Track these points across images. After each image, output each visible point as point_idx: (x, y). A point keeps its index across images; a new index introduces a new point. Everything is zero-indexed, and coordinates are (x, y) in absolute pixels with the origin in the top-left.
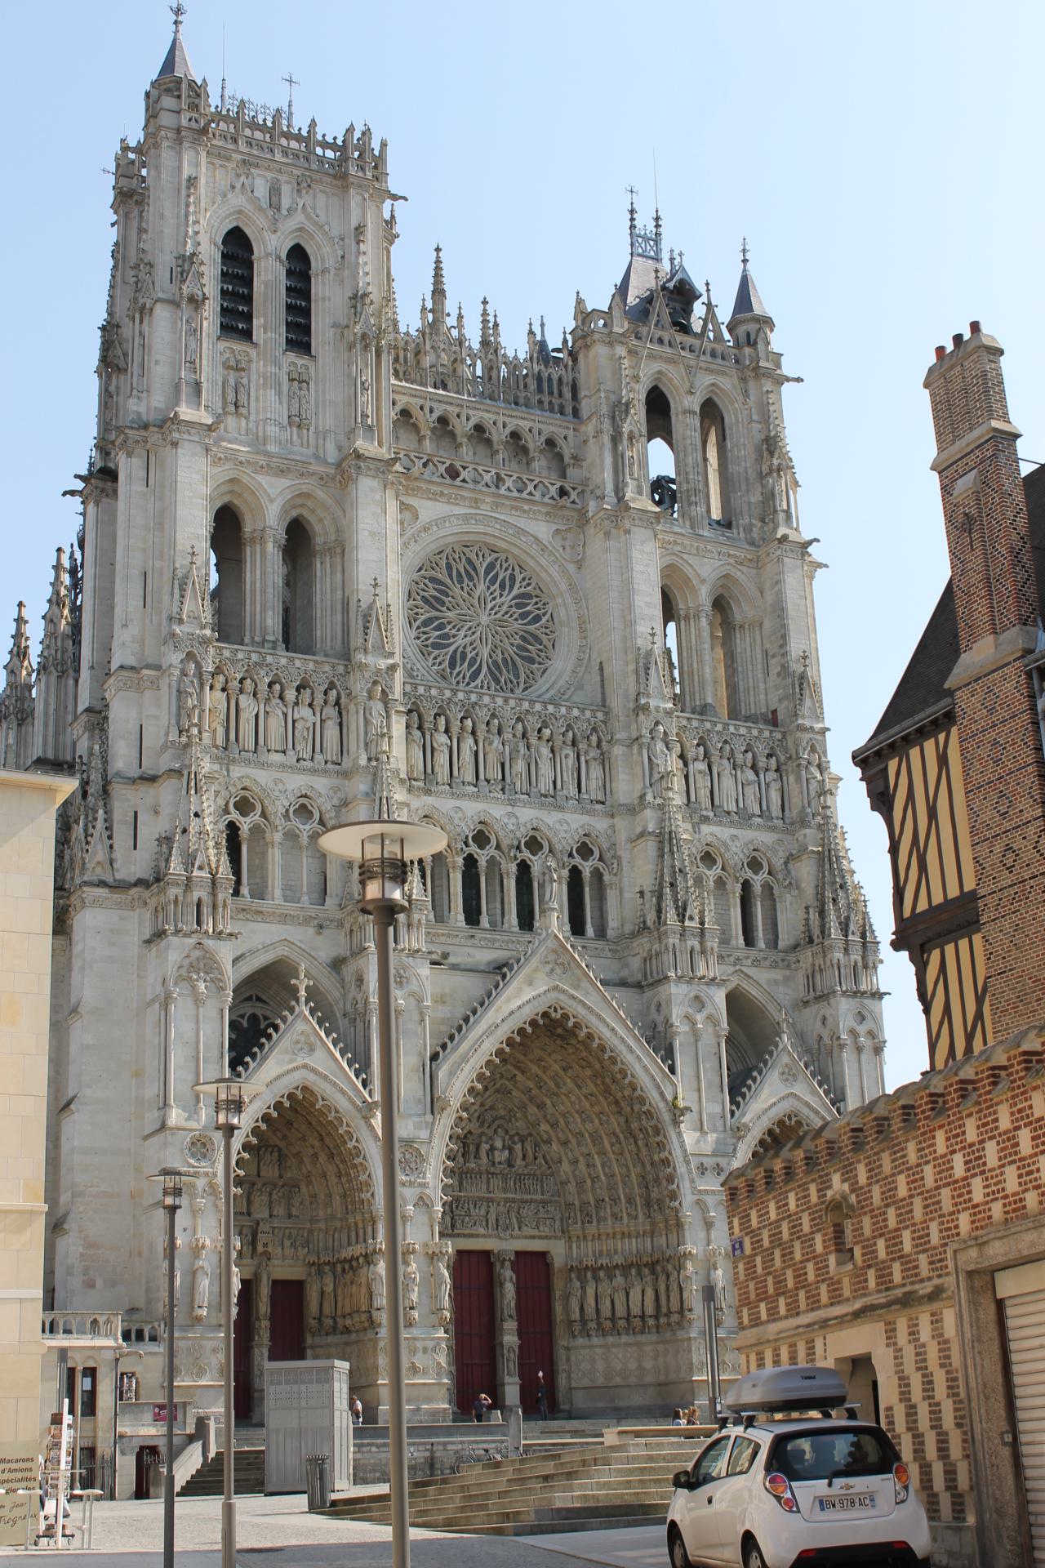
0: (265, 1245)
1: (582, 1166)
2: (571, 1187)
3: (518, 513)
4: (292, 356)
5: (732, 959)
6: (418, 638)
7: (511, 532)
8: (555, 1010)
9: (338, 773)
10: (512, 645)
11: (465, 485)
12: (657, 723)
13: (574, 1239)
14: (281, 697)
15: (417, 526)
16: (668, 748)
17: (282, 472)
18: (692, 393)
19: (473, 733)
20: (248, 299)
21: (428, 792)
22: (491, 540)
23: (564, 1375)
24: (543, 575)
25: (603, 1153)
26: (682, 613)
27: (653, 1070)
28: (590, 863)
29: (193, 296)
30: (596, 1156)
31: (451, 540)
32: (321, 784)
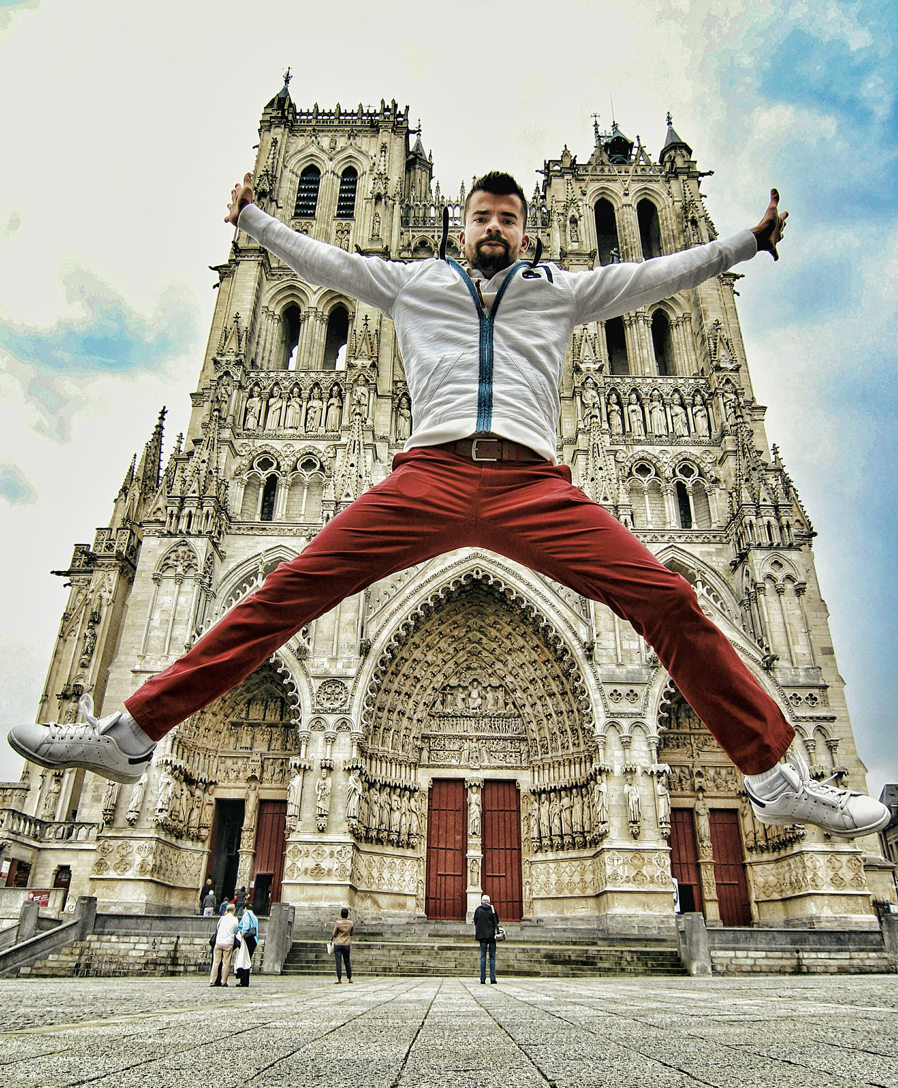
0: (254, 771)
1: (539, 707)
2: (533, 726)
4: (340, 220)
5: (666, 538)
8: (478, 573)
9: (334, 436)
12: (587, 379)
13: (536, 769)
14: (299, 396)
16: (598, 394)
18: (626, 195)
20: (315, 199)
23: (528, 887)
25: (552, 695)
27: (567, 614)
29: (263, 190)
30: (547, 698)
32: (321, 446)
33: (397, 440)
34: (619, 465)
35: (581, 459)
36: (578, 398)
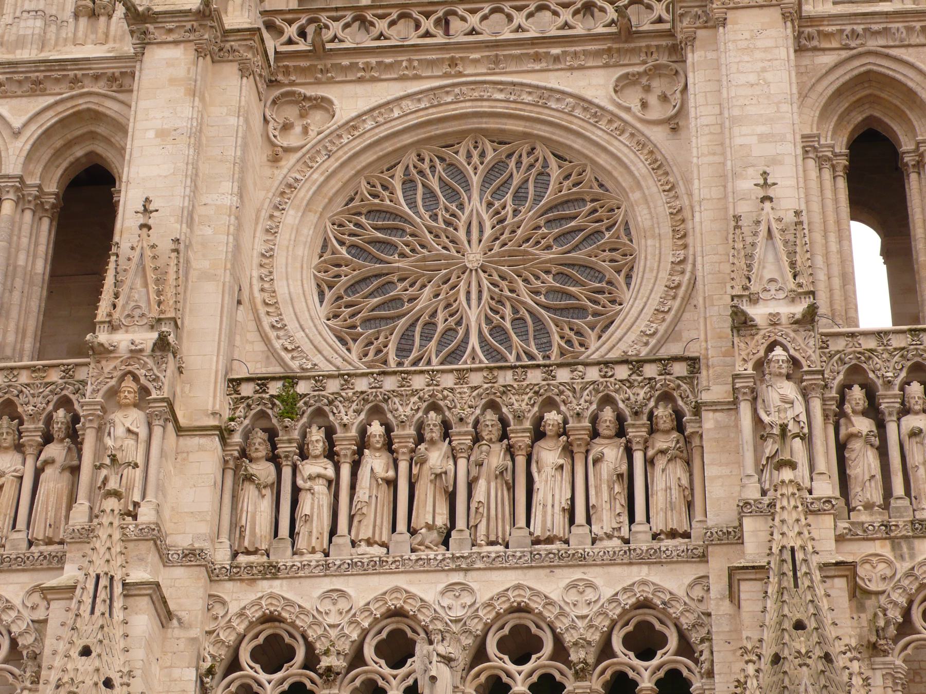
3: (543, 65)
6: (336, 316)
7: (528, 99)
10: (537, 293)
11: (428, 41)
12: (771, 348)
15: (333, 125)
16: (805, 394)
17: (37, 87)
19: (388, 445)
21: (272, 571)
22: (492, 124)
24: (602, 160)
26: (907, 159)
28: (655, 662)
31: (407, 139)
33: (235, 555)
34: (870, 603)
35: (748, 590)
36: (745, 409)
